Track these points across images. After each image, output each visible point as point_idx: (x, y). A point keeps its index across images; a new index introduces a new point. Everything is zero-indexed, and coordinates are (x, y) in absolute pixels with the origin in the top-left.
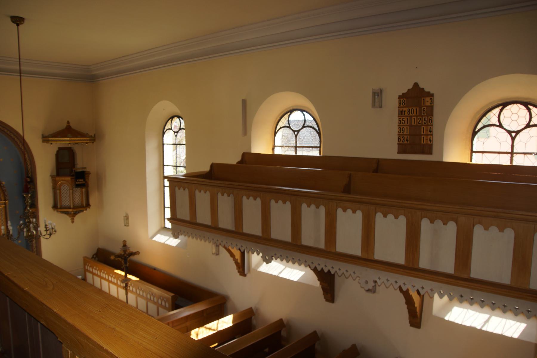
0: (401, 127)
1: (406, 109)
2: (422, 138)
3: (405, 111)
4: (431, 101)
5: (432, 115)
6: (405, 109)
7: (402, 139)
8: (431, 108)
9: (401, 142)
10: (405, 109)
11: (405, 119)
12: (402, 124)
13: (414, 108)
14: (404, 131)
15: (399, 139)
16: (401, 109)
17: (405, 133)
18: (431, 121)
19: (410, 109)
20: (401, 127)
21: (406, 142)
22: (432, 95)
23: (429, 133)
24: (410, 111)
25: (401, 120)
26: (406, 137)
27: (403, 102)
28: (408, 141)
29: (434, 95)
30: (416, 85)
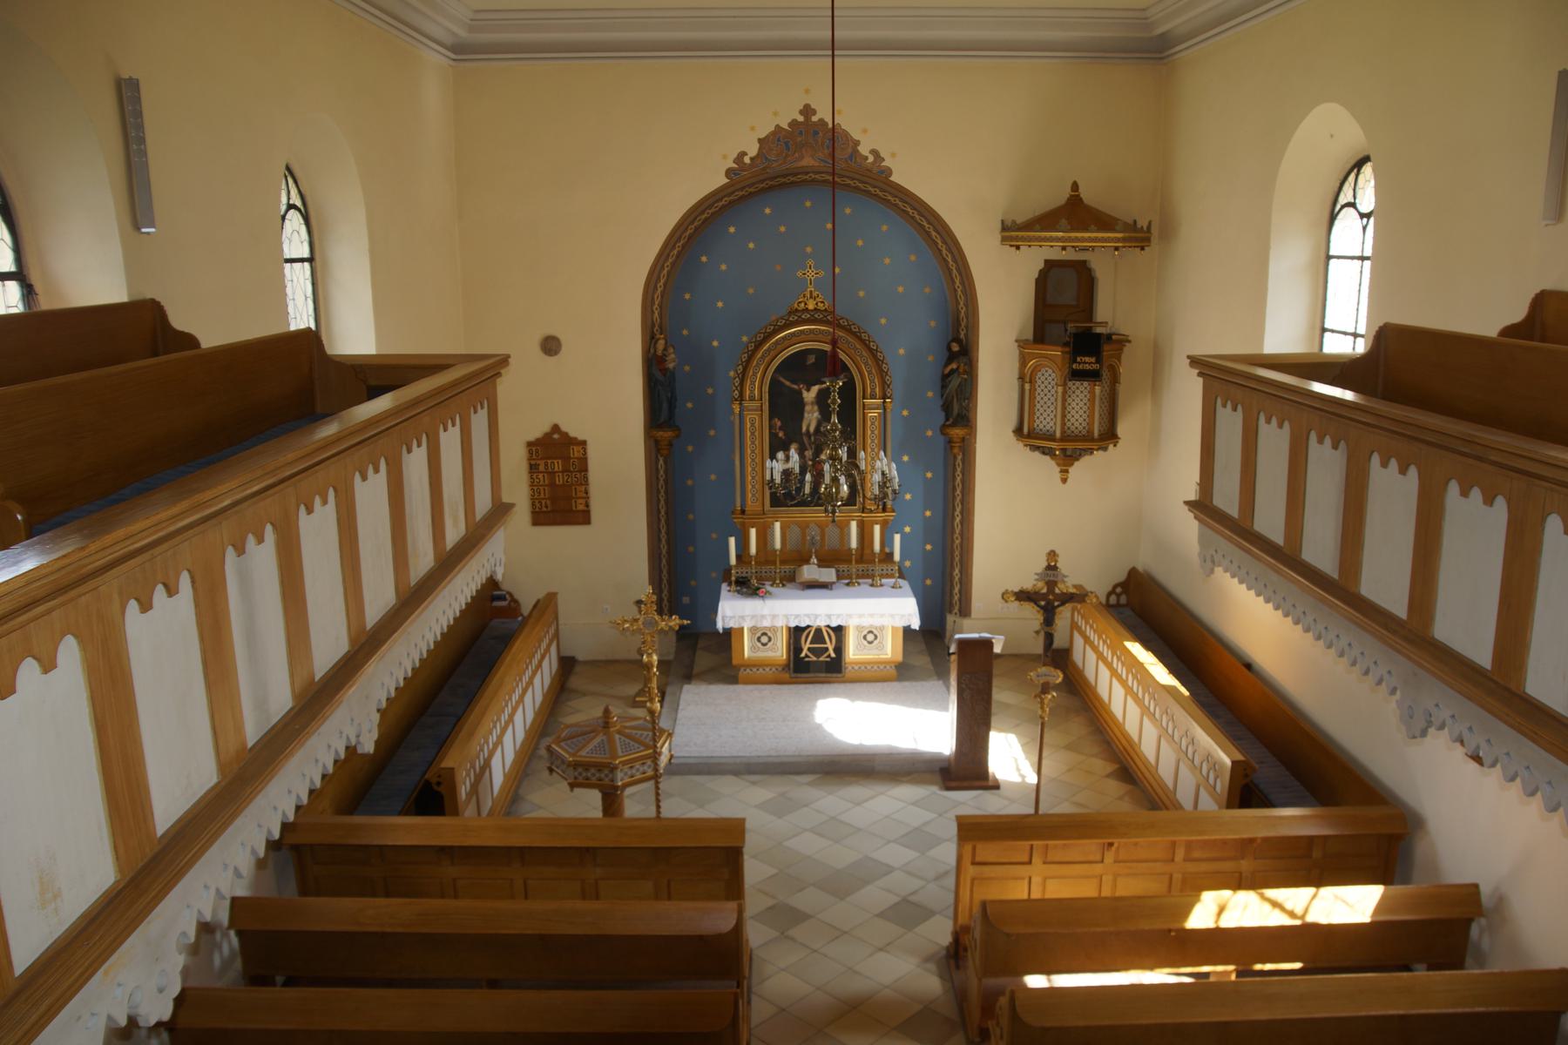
0: (535, 488)
1: (542, 463)
2: (574, 504)
3: (539, 465)
4: (585, 451)
5: (586, 470)
6: (538, 462)
7: (538, 505)
8: (584, 461)
9: (537, 510)
10: (538, 462)
11: (541, 476)
12: (535, 483)
13: (555, 462)
14: (540, 493)
15: (533, 505)
16: (533, 462)
17: (542, 496)
18: (586, 479)
19: (549, 461)
20: (535, 488)
21: (544, 509)
22: (584, 443)
23: (584, 495)
24: (549, 465)
25: (534, 477)
26: (543, 502)
27: (536, 452)
28: (547, 507)
29: (588, 443)
30: (556, 428)
